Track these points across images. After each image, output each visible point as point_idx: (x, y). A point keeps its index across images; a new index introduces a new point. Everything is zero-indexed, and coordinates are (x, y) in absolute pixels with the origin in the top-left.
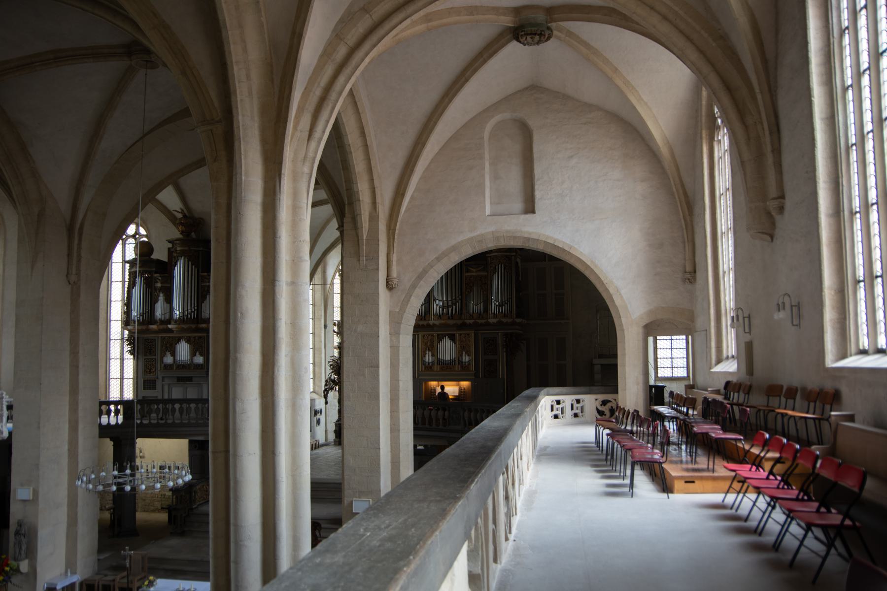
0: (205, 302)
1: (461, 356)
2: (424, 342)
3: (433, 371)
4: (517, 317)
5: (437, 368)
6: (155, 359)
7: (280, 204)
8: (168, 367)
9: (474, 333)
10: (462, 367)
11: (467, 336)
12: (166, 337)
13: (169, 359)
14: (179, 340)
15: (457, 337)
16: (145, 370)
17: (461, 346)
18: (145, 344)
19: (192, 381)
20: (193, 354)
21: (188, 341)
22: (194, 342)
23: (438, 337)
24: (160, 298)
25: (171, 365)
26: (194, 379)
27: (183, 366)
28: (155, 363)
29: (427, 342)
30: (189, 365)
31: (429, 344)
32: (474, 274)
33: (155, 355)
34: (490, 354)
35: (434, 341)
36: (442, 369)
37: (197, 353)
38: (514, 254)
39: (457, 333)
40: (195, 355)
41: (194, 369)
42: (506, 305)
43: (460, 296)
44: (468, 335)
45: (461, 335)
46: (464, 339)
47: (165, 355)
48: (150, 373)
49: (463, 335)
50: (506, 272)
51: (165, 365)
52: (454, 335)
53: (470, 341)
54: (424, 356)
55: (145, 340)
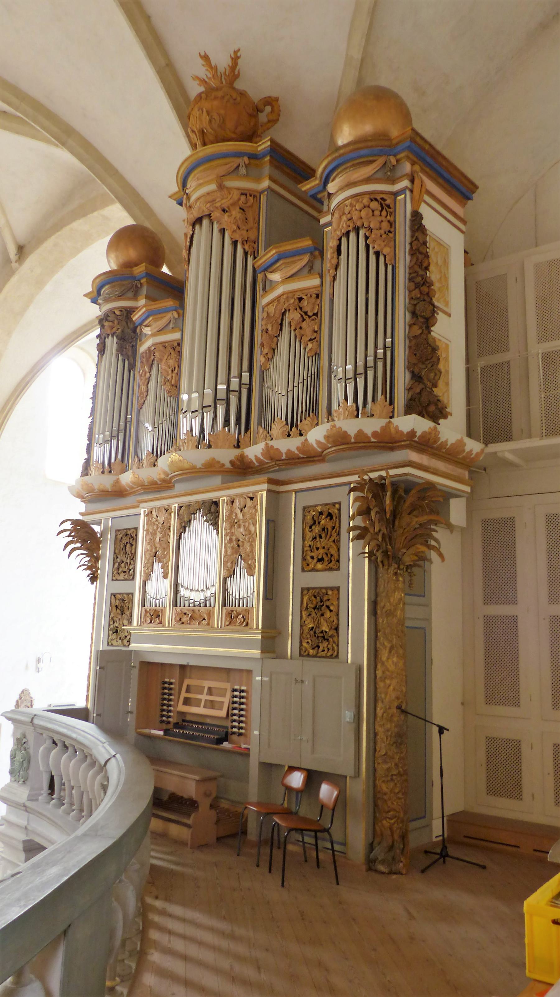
1: (232, 573)
2: (147, 530)
3: (164, 626)
4: (408, 410)
5: (169, 616)
7: (40, 283)
9: (269, 491)
10: (230, 614)
11: (249, 503)
15: (223, 510)
17: (231, 540)
23: (178, 515)
29: (155, 534)
31: (159, 535)
32: (279, 291)
34: (319, 566)
35: (170, 529)
36: (180, 621)
38: (405, 183)
39: (223, 496)
42: (370, 373)
43: (245, 375)
44: (252, 499)
45: (232, 502)
46: (240, 516)
49: (237, 504)
50: (372, 258)
52: (216, 504)
53: (254, 525)
54: (148, 577)
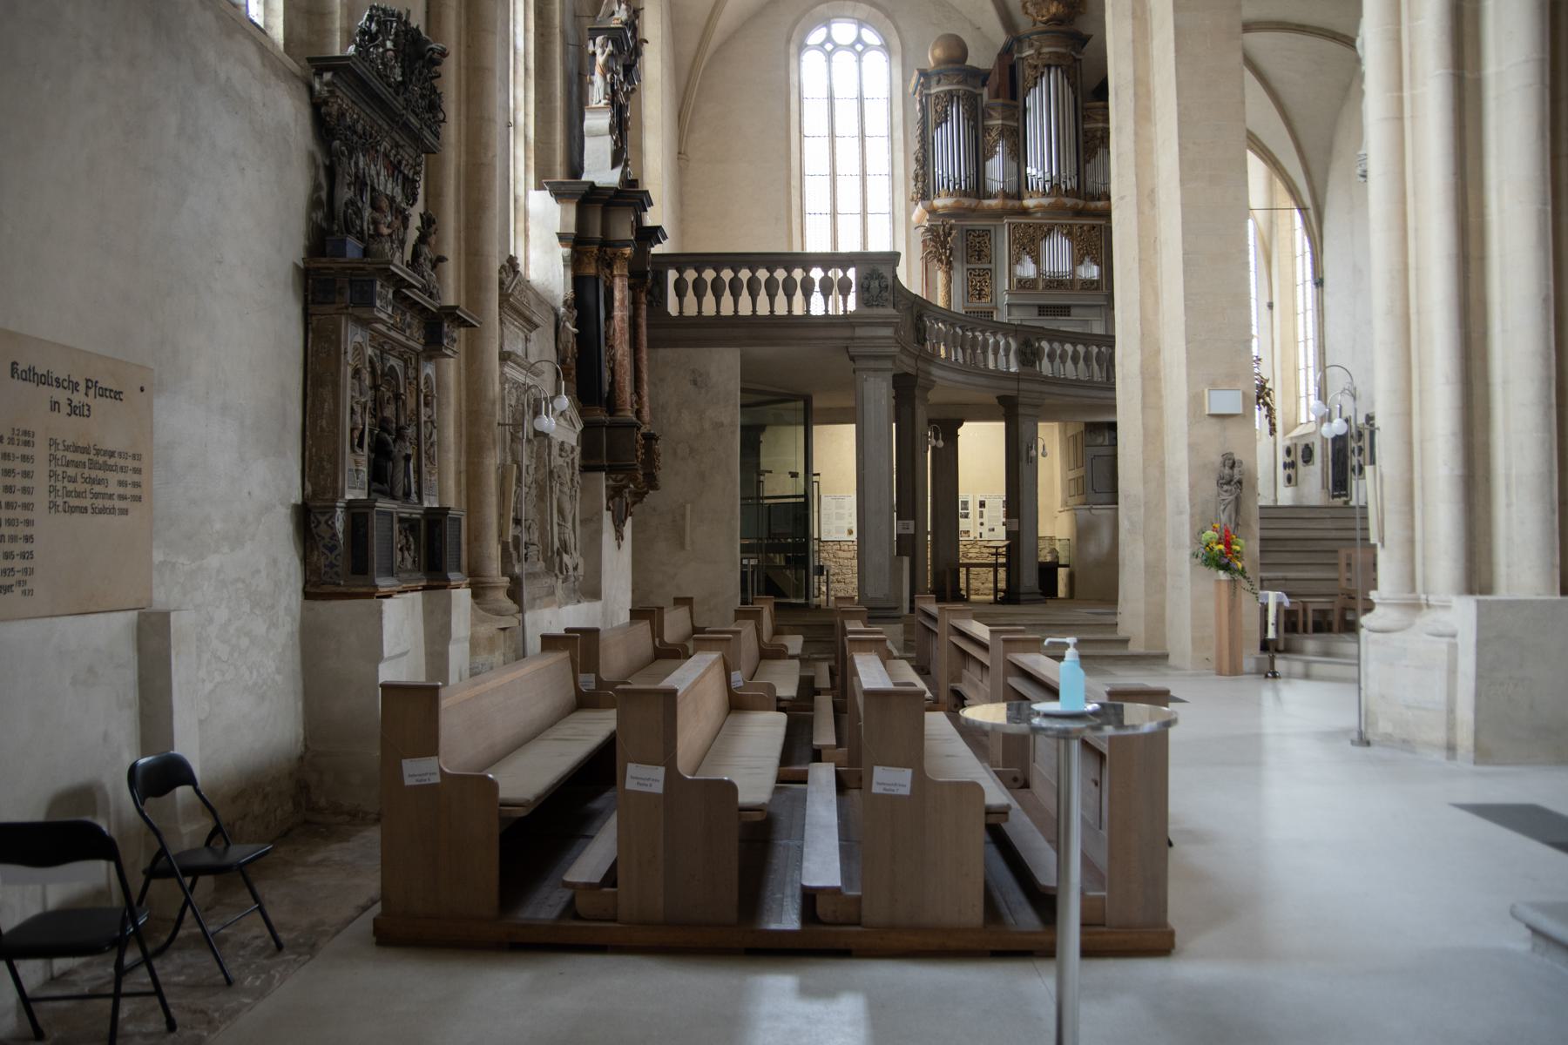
0: (1092, 161)
6: (990, 270)
8: (1024, 284)
12: (1020, 224)
13: (1028, 270)
14: (1048, 232)
16: (968, 292)
18: (967, 240)
19: (1069, 315)
20: (1077, 261)
21: (1069, 234)
22: (1081, 235)
24: (999, 149)
25: (1032, 279)
26: (1073, 311)
27: (1056, 283)
28: (990, 279)
30: (1072, 282)
33: (990, 262)
37: (1087, 259)
40: (1081, 263)
41: (1081, 289)
47: (1018, 261)
48: (980, 299)
51: (1020, 281)
55: (967, 231)
